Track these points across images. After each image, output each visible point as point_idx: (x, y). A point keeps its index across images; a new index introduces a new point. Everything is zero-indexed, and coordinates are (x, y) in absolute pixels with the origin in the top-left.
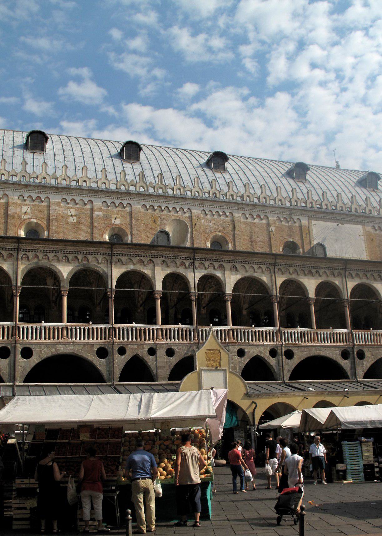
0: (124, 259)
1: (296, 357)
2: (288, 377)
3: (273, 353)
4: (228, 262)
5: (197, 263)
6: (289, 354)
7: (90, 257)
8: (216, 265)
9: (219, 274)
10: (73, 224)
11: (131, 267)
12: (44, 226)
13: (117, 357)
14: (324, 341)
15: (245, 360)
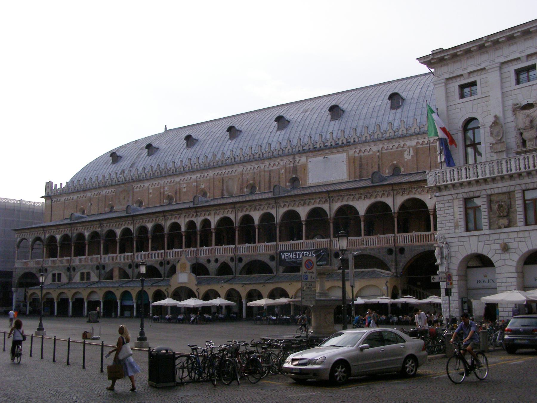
0: (170, 217)
1: (244, 261)
2: (239, 271)
3: (232, 259)
4: (213, 210)
5: (199, 214)
6: (240, 260)
7: (158, 219)
8: (207, 213)
9: (209, 218)
10: (184, 192)
11: (173, 221)
12: (173, 196)
13: (166, 265)
14: (261, 250)
15: (218, 265)
